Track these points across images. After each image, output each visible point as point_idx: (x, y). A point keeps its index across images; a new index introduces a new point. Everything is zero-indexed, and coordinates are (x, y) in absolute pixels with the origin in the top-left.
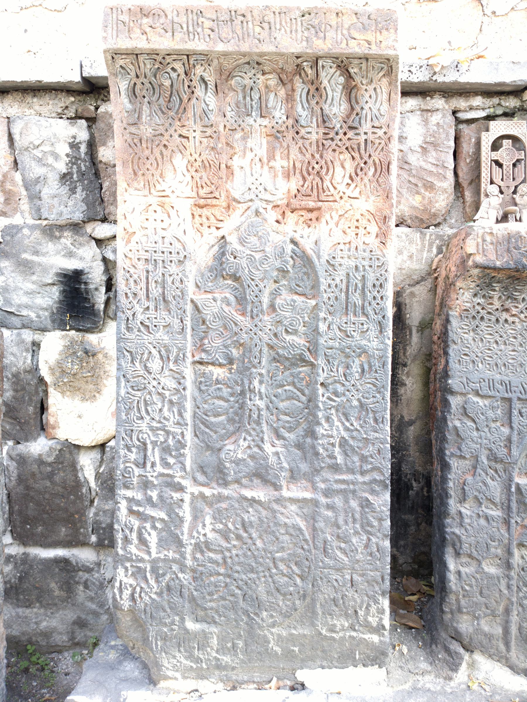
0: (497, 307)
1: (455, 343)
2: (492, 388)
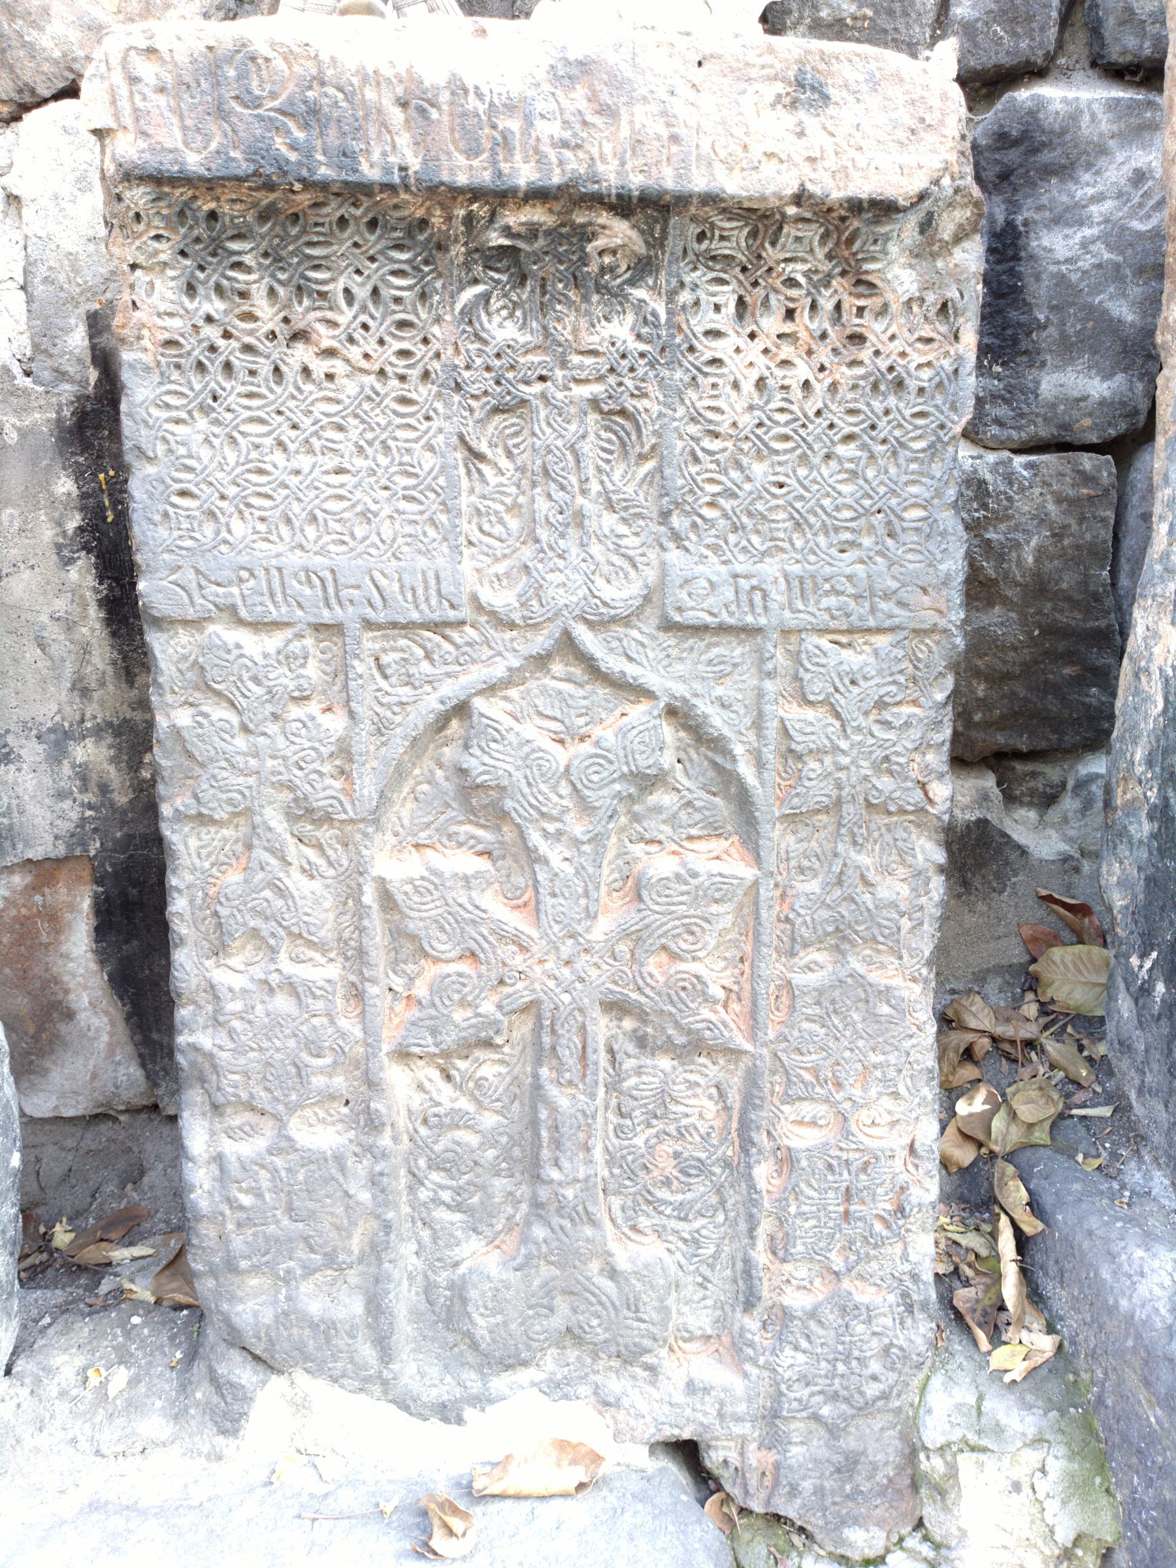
0: (270, 326)
1: (149, 459)
2: (279, 597)
